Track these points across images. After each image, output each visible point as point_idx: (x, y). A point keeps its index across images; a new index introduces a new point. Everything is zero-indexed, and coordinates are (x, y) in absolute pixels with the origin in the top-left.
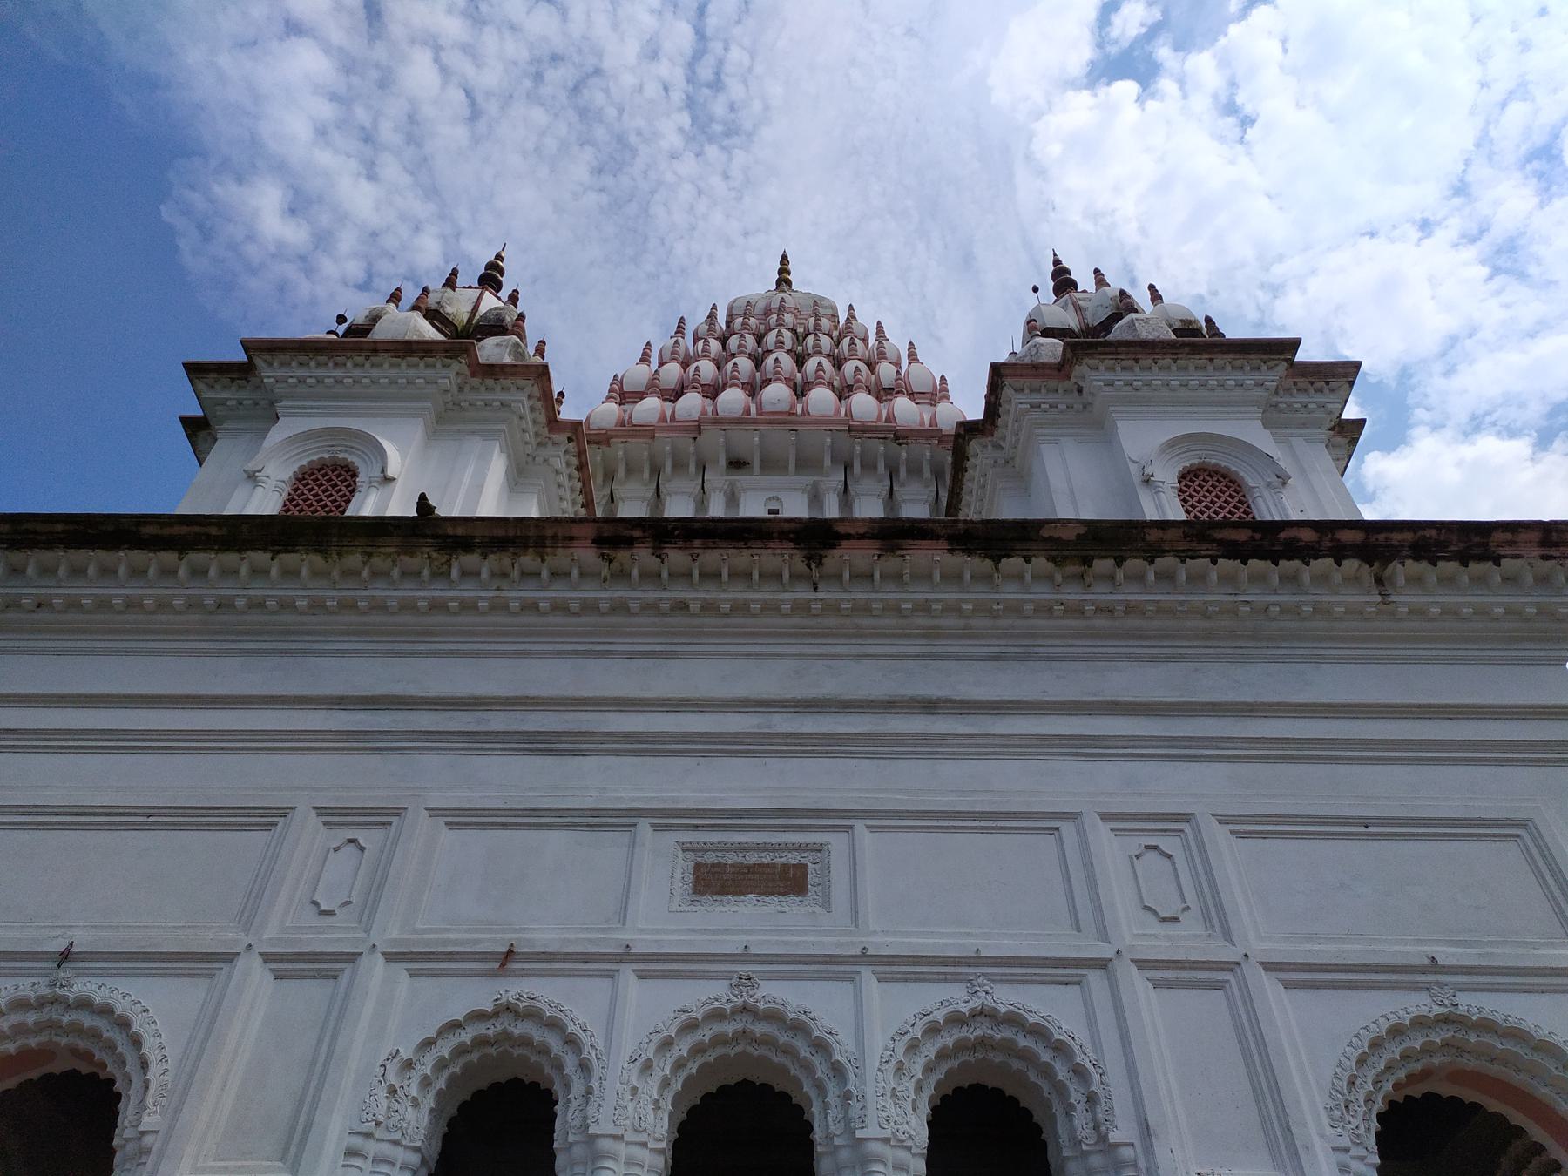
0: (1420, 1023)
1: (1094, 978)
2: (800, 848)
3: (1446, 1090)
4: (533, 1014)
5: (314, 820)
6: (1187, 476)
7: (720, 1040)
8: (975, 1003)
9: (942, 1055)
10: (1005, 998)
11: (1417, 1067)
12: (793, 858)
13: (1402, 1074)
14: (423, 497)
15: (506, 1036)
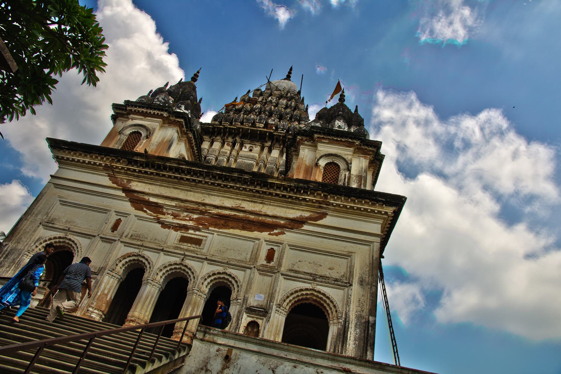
0: (307, 289)
1: (248, 271)
2: (203, 236)
3: (314, 303)
4: (143, 257)
5: (114, 214)
6: (327, 164)
7: (175, 268)
8: (224, 271)
9: (215, 279)
10: (229, 271)
11: (304, 297)
12: (201, 238)
13: (300, 298)
14: (146, 149)
15: (138, 260)
